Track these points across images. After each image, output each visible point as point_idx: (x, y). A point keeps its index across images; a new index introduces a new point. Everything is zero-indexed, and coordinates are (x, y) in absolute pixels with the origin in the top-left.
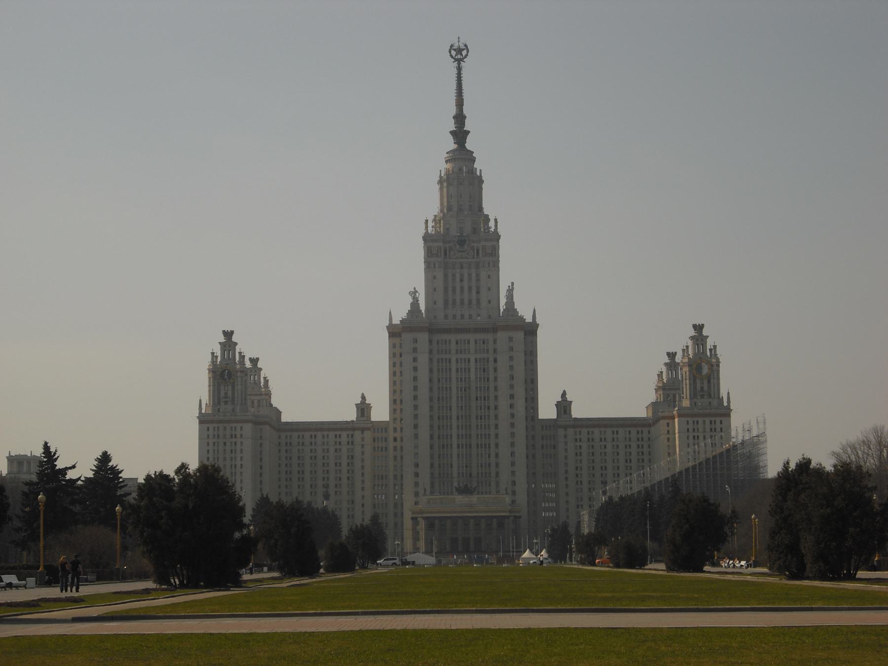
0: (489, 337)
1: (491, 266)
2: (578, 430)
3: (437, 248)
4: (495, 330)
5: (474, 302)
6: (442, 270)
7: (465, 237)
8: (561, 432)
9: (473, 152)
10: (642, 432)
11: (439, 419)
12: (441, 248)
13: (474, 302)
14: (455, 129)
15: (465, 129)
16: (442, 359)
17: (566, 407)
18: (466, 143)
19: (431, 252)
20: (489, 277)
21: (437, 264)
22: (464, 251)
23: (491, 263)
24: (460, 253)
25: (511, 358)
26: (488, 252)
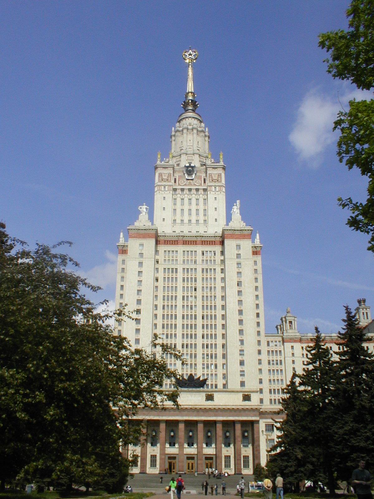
1: (217, 190)
3: (167, 175)
4: (222, 243)
5: (201, 221)
6: (171, 192)
7: (193, 167)
8: (288, 345)
12: (171, 175)
20: (215, 198)
21: (167, 187)
23: (217, 187)
24: (188, 181)
26: (215, 178)
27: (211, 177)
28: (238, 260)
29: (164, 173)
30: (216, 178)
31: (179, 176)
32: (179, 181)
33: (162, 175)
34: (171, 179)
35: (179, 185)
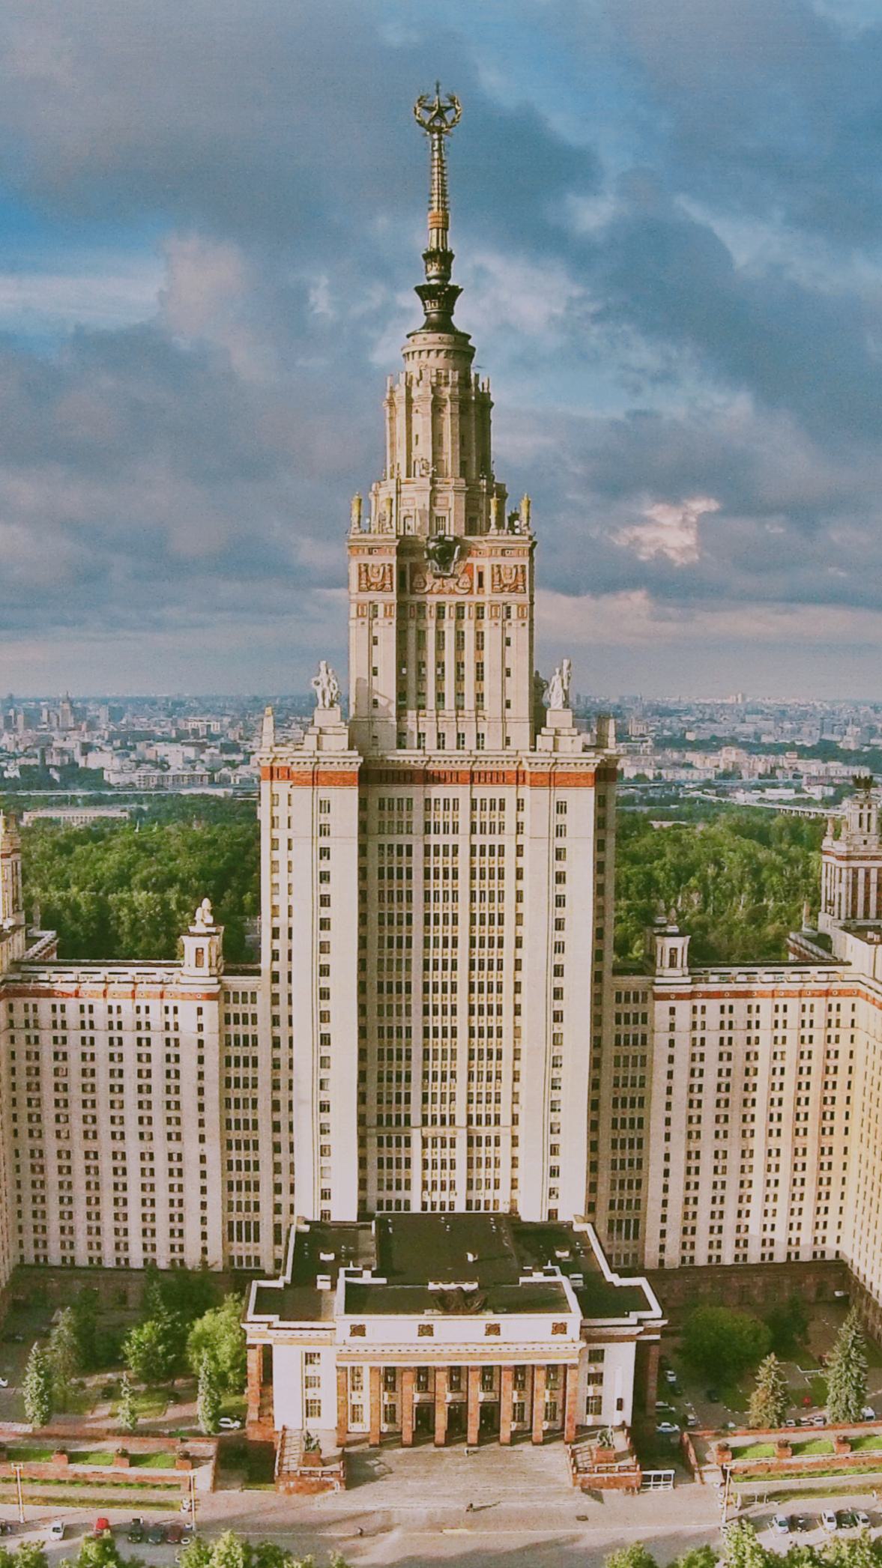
0: (507, 793)
2: (699, 1003)
5: (469, 702)
6: (394, 621)
9: (469, 337)
10: (838, 1006)
11: (380, 990)
13: (469, 702)
14: (427, 283)
15: (451, 283)
16: (391, 847)
17: (676, 949)
18: (452, 314)
19: (368, 580)
22: (445, 577)
24: (437, 581)
25: (560, 854)
27: (497, 578)
28: (560, 842)
29: (375, 563)
30: (510, 582)
31: (411, 564)
32: (412, 581)
33: (366, 571)
34: (391, 584)
35: (413, 592)
